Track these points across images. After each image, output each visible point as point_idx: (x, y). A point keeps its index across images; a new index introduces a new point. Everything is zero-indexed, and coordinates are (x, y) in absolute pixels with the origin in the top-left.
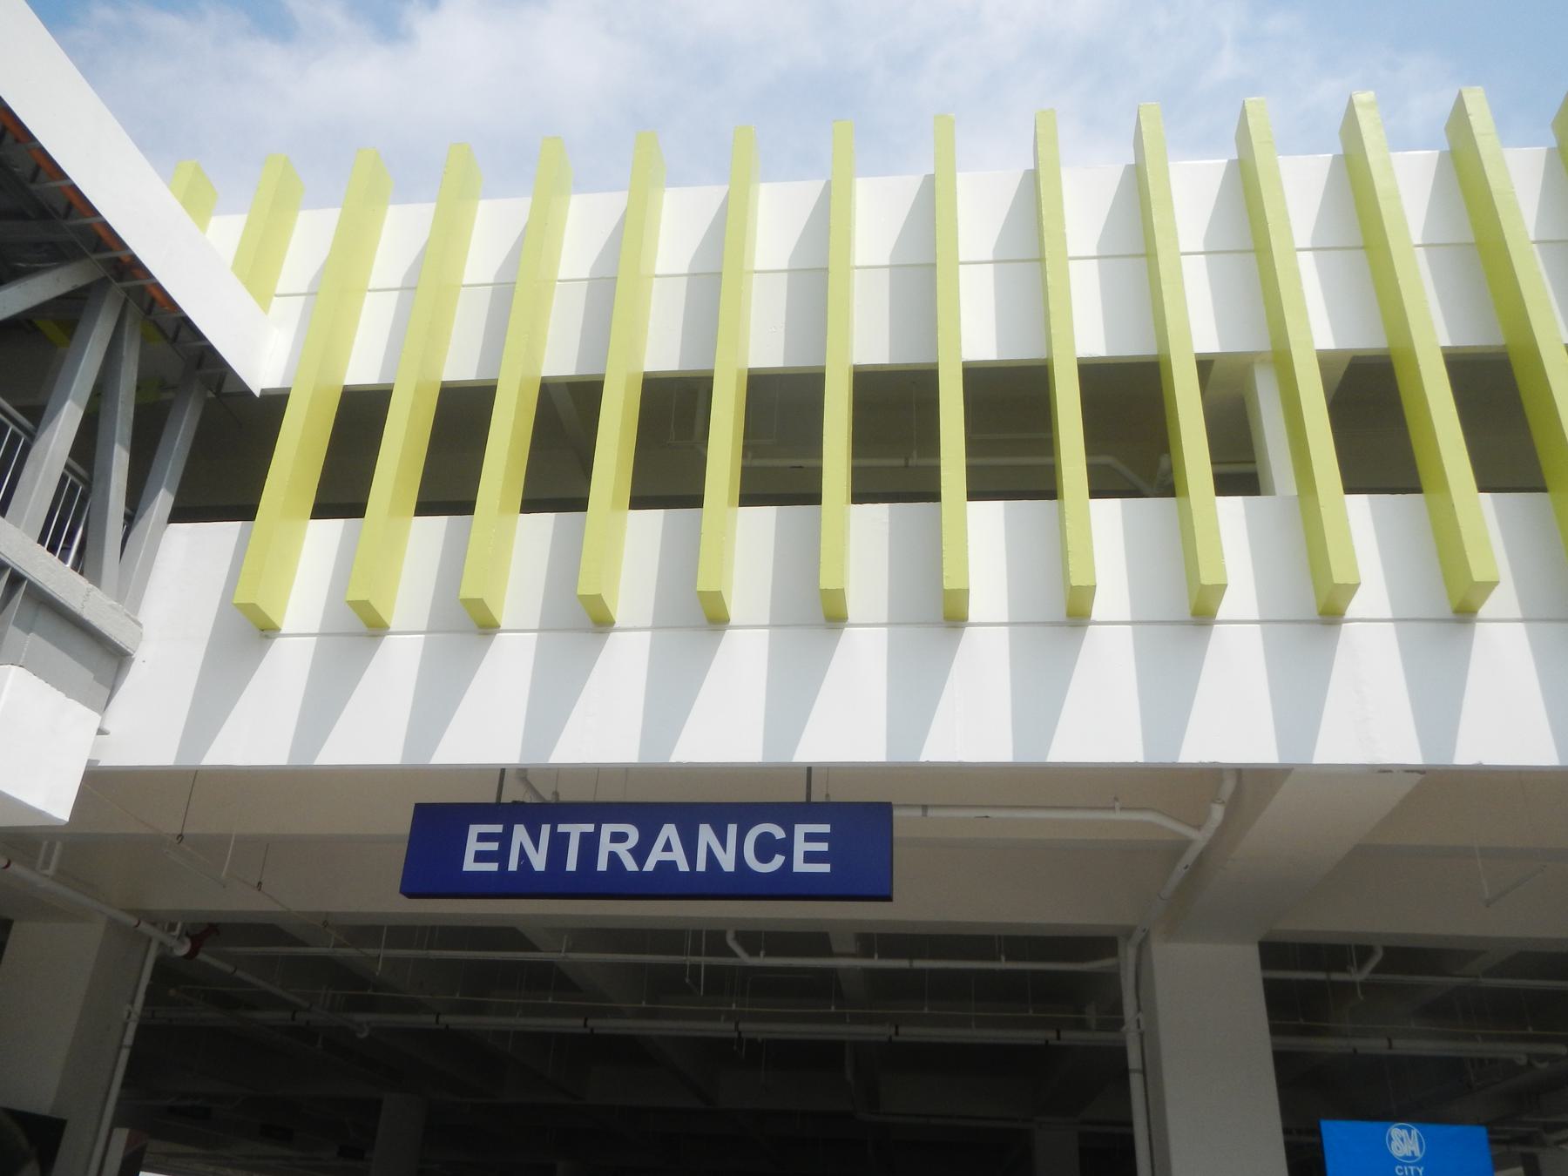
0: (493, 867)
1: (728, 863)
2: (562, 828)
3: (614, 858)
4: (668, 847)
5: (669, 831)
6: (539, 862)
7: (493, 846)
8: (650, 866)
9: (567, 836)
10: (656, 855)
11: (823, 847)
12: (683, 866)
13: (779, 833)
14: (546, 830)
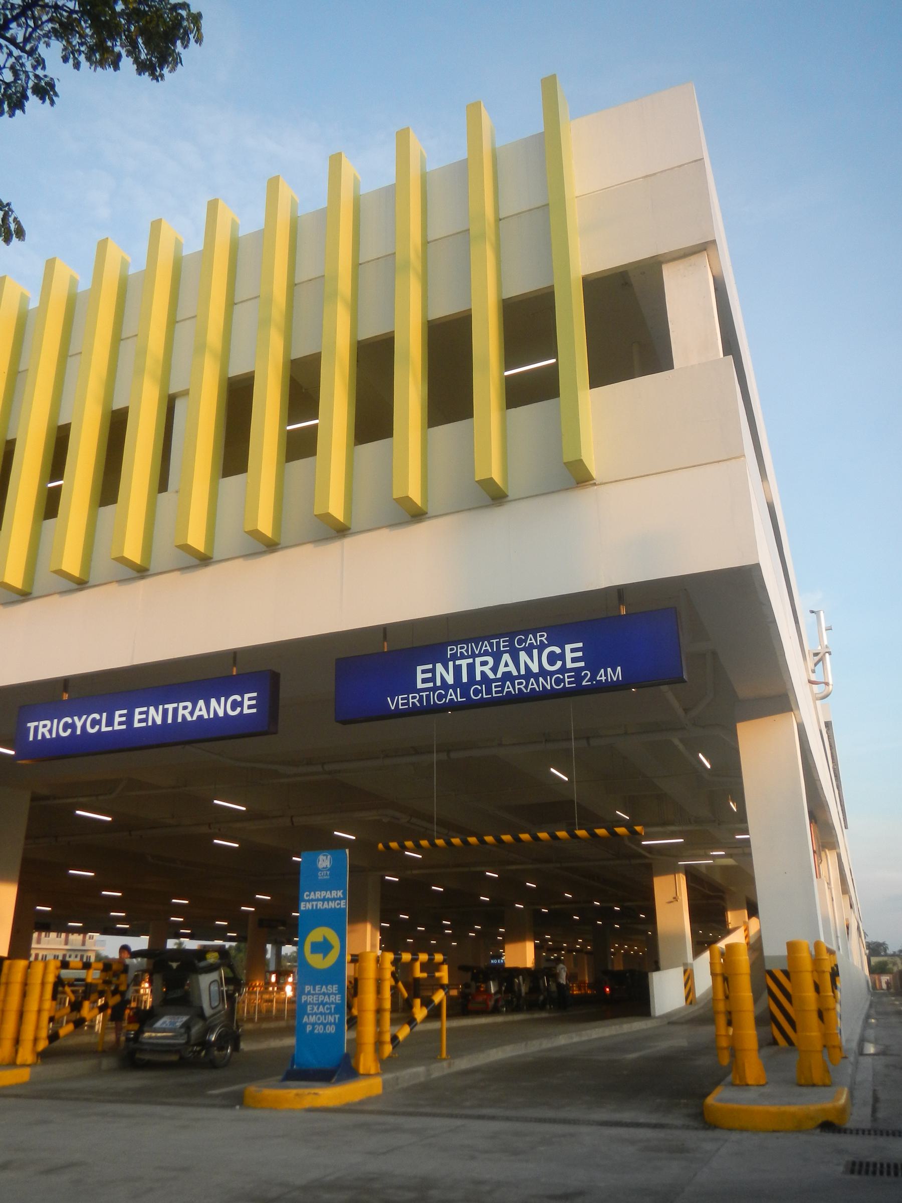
0: (144, 724)
1: (221, 714)
2: (166, 706)
3: (183, 716)
4: (200, 710)
5: (201, 703)
6: (159, 721)
7: (144, 716)
8: (195, 718)
10: (197, 713)
11: (254, 702)
12: (206, 717)
13: (238, 698)
14: (161, 707)
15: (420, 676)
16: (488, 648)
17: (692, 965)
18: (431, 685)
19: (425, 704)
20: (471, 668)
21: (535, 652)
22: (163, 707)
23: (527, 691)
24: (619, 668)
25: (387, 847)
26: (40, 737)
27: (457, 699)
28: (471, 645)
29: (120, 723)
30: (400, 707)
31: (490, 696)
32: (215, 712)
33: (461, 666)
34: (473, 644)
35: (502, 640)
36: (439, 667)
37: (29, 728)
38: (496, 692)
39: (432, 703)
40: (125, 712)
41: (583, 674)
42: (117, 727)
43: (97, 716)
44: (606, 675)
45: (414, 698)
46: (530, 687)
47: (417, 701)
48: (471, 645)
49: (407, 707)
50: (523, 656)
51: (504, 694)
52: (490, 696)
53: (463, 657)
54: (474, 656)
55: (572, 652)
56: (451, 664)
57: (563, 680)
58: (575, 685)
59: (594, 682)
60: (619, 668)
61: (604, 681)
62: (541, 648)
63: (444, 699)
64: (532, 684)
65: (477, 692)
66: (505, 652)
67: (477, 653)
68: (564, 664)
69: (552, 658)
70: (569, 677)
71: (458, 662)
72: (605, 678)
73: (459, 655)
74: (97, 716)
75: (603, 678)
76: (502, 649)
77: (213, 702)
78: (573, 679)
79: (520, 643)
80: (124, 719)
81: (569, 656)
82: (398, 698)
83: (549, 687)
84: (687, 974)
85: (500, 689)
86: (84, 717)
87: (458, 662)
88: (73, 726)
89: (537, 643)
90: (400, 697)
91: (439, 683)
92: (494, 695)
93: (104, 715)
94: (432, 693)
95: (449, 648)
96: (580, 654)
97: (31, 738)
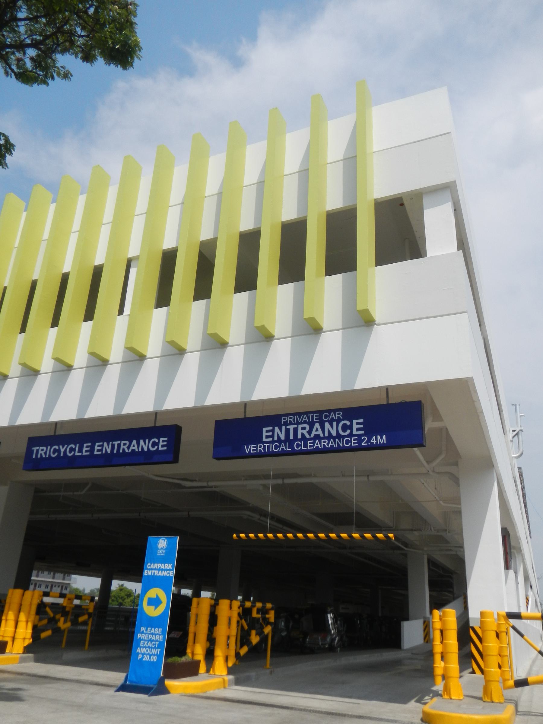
0: (100, 453)
1: (146, 449)
2: (114, 443)
3: (124, 449)
4: (134, 446)
5: (134, 442)
7: (100, 448)
8: (130, 451)
9: (114, 444)
10: (132, 448)
11: (165, 443)
12: (137, 450)
13: (156, 440)
14: (111, 443)
15: (265, 434)
16: (307, 419)
17: (429, 618)
18: (271, 439)
19: (267, 451)
20: (296, 431)
21: (335, 423)
22: (112, 443)
23: (328, 446)
24: (384, 436)
25: (238, 536)
26: (39, 456)
27: (286, 449)
28: (297, 417)
29: (86, 451)
30: (252, 452)
31: (306, 448)
32: (142, 448)
33: (289, 429)
34: (297, 416)
35: (315, 415)
36: (277, 429)
37: (34, 450)
38: (310, 446)
39: (271, 451)
40: (89, 444)
41: (362, 439)
42: (84, 453)
43: (73, 446)
44: (376, 440)
45: (260, 447)
46: (330, 444)
47: (262, 449)
48: (297, 417)
49: (256, 452)
50: (327, 425)
51: (315, 448)
52: (306, 448)
53: (291, 424)
54: (298, 423)
55: (356, 424)
56: (284, 428)
57: (351, 442)
58: (357, 445)
59: (369, 444)
60: (384, 436)
61: (375, 443)
62: (338, 421)
63: (278, 449)
64: (332, 443)
65: (298, 446)
66: (317, 422)
67: (300, 422)
68: (352, 432)
69: (345, 428)
70: (354, 440)
71: (288, 427)
72: (376, 441)
73: (289, 423)
74: (73, 446)
75: (375, 442)
76: (315, 420)
77: (142, 442)
78: (357, 441)
79: (326, 417)
80: (88, 449)
81: (355, 427)
82: (251, 446)
83: (342, 445)
84: (426, 624)
85: (312, 444)
86: (66, 446)
87: (288, 427)
88: (59, 451)
89: (336, 418)
90: (252, 446)
91: (276, 439)
92: (308, 448)
93: (78, 445)
94: (271, 444)
95: (283, 418)
96: (361, 426)
97: (34, 457)
